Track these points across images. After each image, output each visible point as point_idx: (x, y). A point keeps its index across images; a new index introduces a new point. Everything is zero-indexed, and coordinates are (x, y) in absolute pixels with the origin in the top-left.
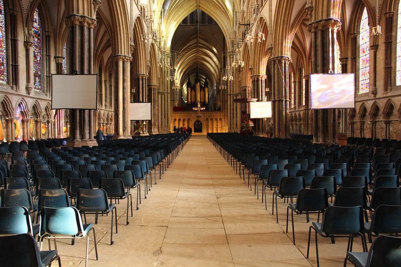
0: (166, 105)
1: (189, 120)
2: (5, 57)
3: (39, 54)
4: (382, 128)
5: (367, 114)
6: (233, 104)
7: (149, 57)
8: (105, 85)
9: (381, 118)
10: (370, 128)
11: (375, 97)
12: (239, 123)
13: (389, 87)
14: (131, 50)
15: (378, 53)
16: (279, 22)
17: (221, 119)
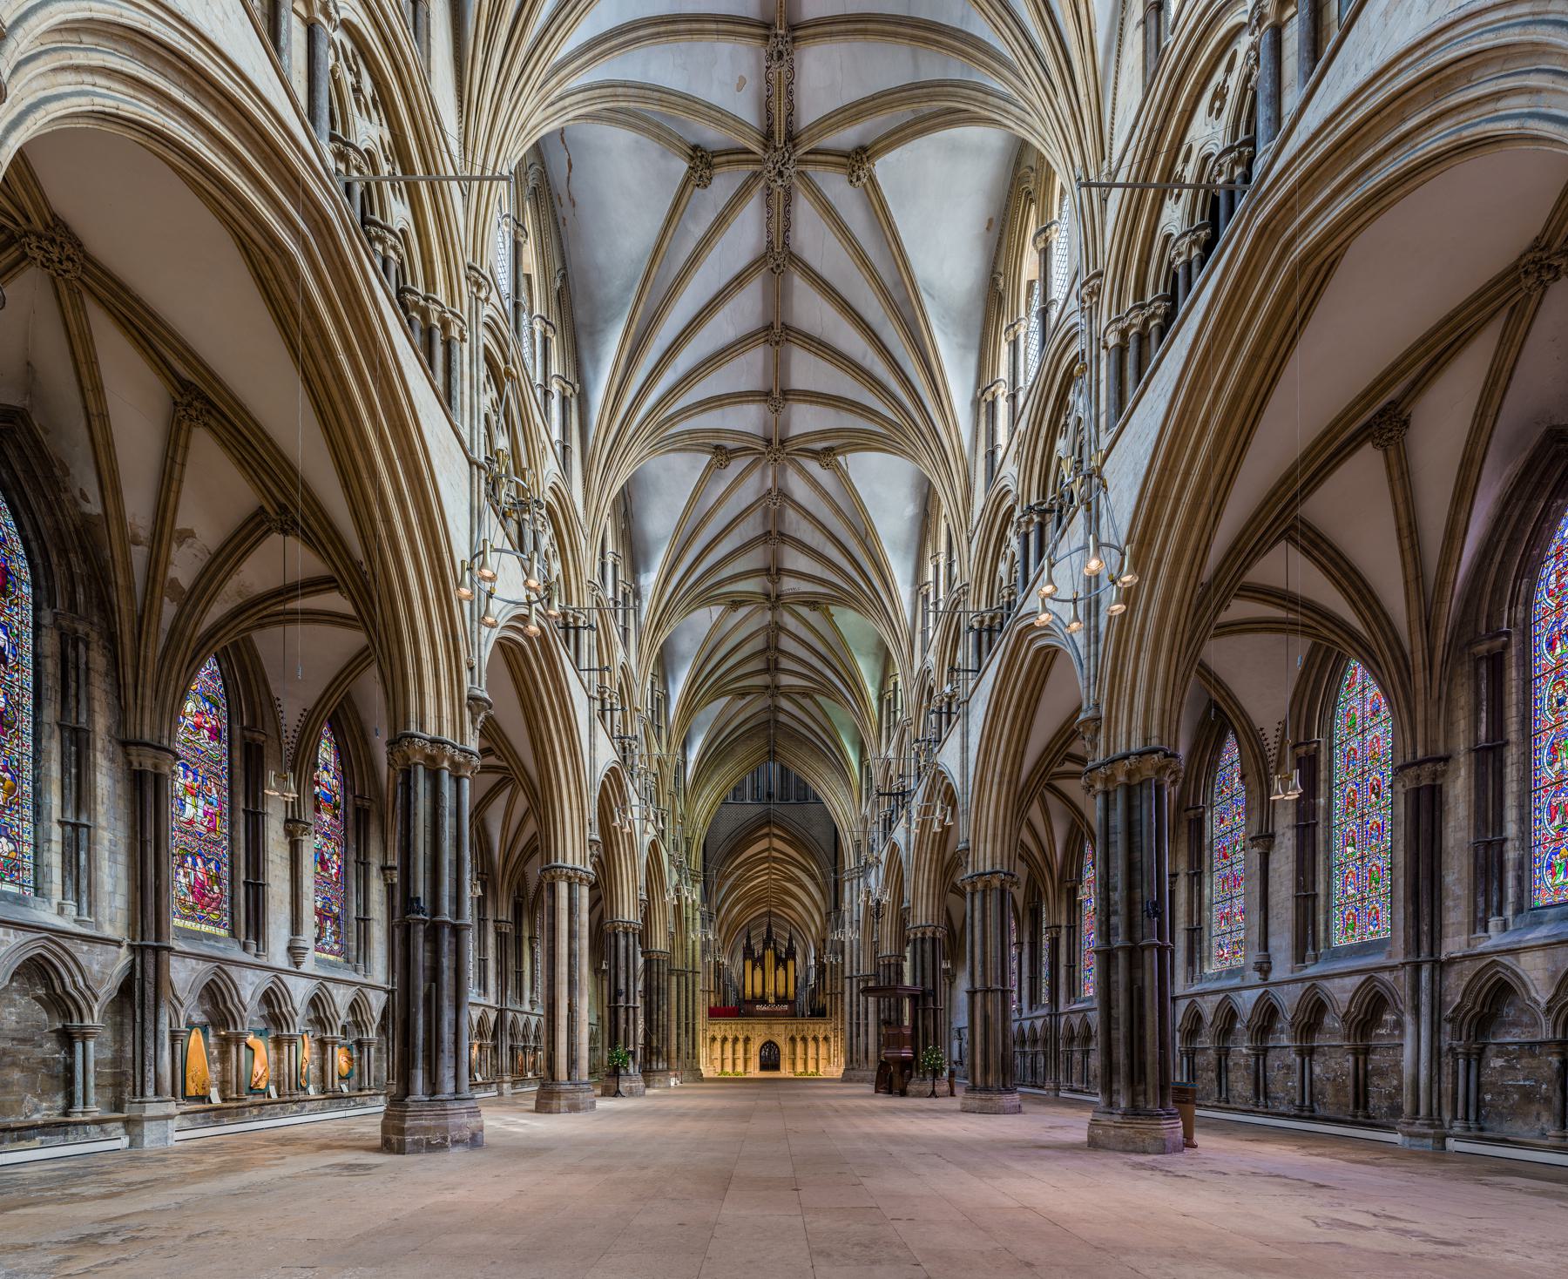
0: (690, 1003)
1: (747, 1040)
2: (226, 860)
3: (335, 857)
4: (1288, 1067)
5: (1238, 1026)
6: (858, 1001)
7: (643, 878)
8: (532, 949)
9: (1284, 1038)
10: (1247, 1067)
11: (1265, 979)
12: (872, 1048)
13: (1310, 952)
14: (591, 855)
15: (1273, 857)
16: (989, 778)
17: (826, 1039)
